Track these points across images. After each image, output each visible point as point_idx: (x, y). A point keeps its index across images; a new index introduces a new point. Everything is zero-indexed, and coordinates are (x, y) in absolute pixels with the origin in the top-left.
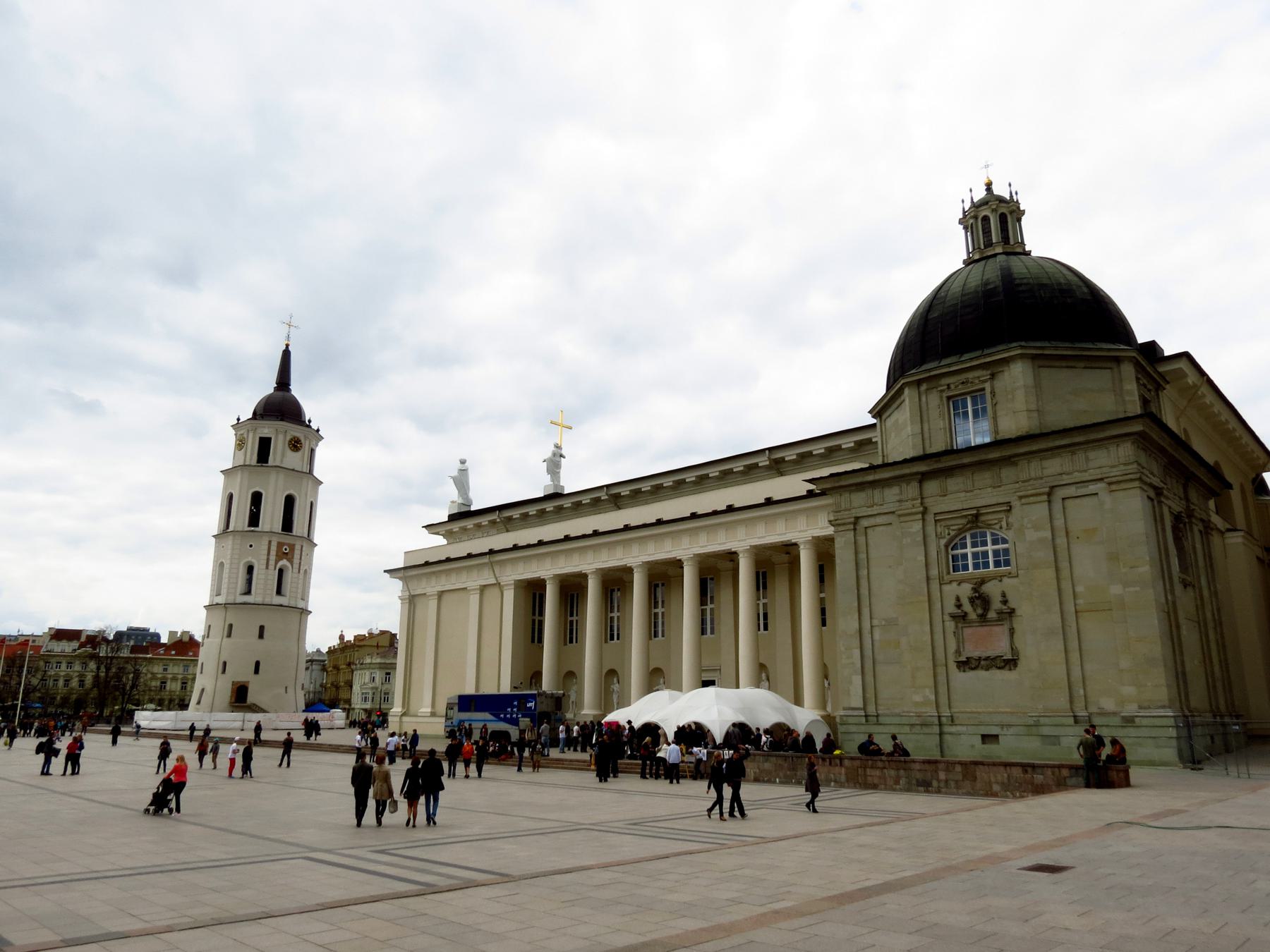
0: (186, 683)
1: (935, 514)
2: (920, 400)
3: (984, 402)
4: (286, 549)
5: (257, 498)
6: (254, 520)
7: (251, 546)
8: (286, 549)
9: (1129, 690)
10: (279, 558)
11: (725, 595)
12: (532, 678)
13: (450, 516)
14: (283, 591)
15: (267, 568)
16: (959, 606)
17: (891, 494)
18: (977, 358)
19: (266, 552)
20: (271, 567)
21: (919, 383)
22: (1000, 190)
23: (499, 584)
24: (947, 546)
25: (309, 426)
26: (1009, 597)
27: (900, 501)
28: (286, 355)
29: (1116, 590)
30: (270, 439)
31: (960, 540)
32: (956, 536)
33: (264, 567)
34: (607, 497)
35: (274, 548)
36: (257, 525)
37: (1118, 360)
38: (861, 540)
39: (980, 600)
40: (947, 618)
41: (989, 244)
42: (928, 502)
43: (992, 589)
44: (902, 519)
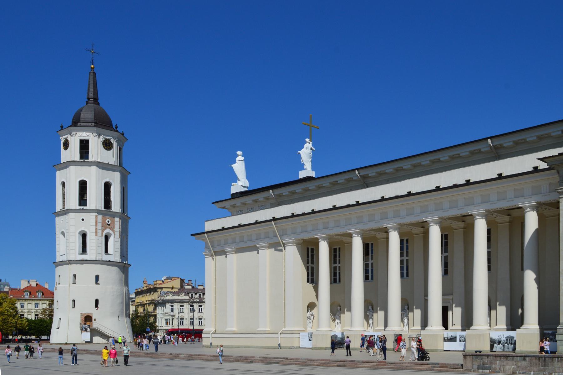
5: (83, 186)
14: (109, 252)
15: (96, 235)
19: (94, 224)
20: (99, 234)
30: (87, 141)
33: (94, 234)
35: (100, 221)
36: (86, 205)
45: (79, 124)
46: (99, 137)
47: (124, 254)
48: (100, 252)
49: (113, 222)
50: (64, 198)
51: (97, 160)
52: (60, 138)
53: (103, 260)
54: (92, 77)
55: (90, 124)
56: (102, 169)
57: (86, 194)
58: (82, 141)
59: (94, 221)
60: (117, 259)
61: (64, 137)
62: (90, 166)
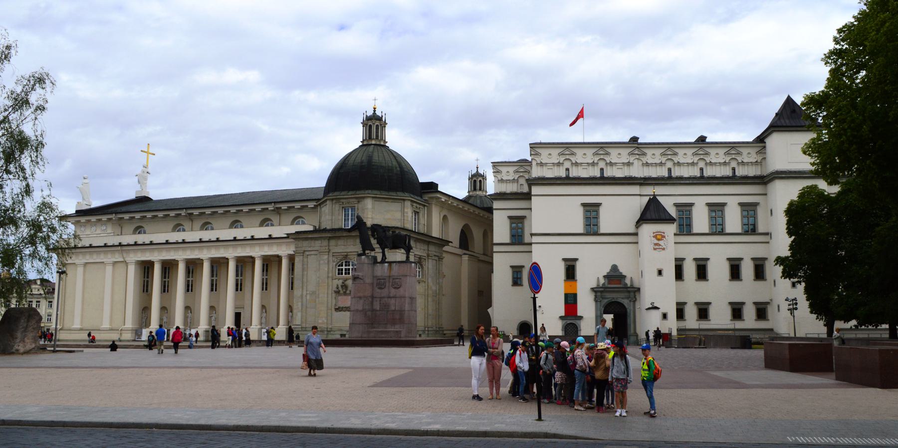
1: (333, 253)
2: (332, 207)
3: (355, 211)
11: (248, 274)
12: (143, 310)
13: (77, 212)
16: (338, 288)
17: (318, 243)
18: (353, 195)
21: (332, 200)
22: (378, 113)
23: (126, 261)
24: (336, 265)
27: (321, 246)
32: (339, 262)
34: (184, 214)
37: (404, 200)
38: (305, 260)
39: (345, 286)
40: (333, 292)
41: (370, 138)
42: (331, 248)
44: (321, 254)
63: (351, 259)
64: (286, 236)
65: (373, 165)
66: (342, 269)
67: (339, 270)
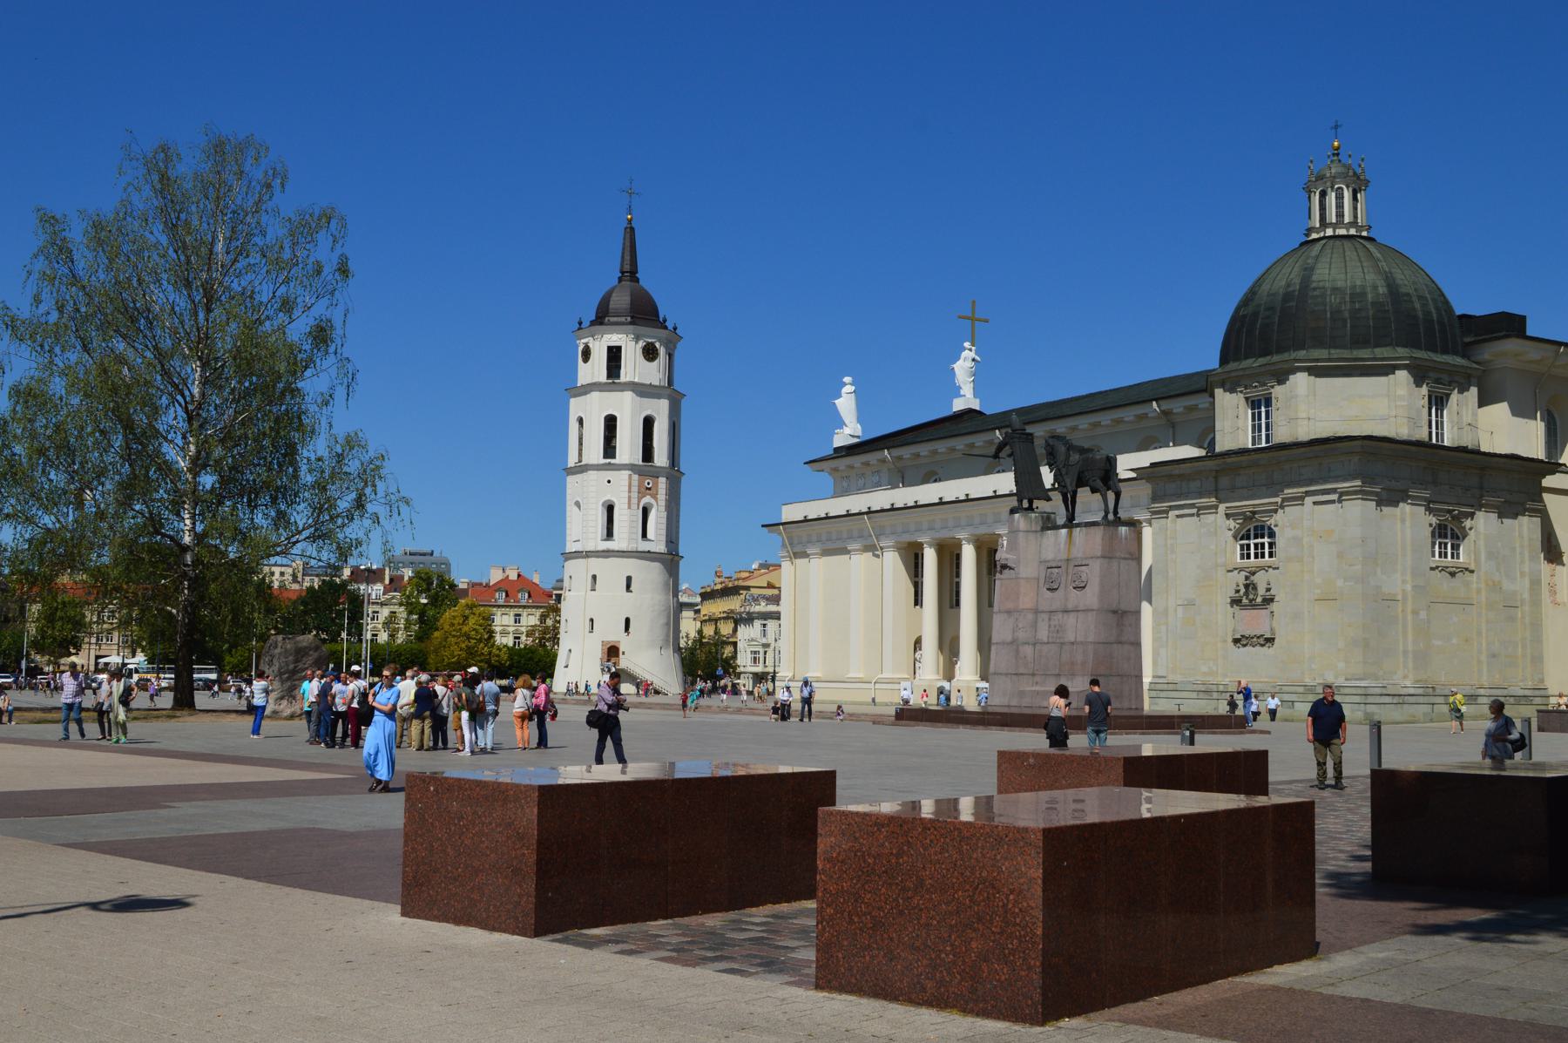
0: (519, 638)
4: (648, 484)
5: (611, 423)
6: (609, 449)
7: (609, 482)
8: (648, 484)
9: (1341, 665)
10: (641, 495)
15: (629, 507)
25: (666, 328)
26: (1272, 586)
28: (630, 231)
29: (1340, 583)
30: (619, 349)
31: (1247, 531)
36: (614, 457)
39: (1250, 587)
43: (1260, 579)
45: (607, 319)
46: (637, 342)
47: (672, 539)
48: (634, 536)
49: (656, 484)
50: (581, 444)
51: (632, 380)
52: (578, 342)
53: (640, 549)
54: (628, 236)
55: (623, 319)
56: (641, 396)
57: (615, 437)
58: (610, 349)
59: (627, 483)
60: (660, 547)
61: (582, 341)
62: (622, 391)
63: (1263, 521)
64: (1133, 475)
65: (1315, 289)
66: (1263, 545)
67: (1242, 546)
